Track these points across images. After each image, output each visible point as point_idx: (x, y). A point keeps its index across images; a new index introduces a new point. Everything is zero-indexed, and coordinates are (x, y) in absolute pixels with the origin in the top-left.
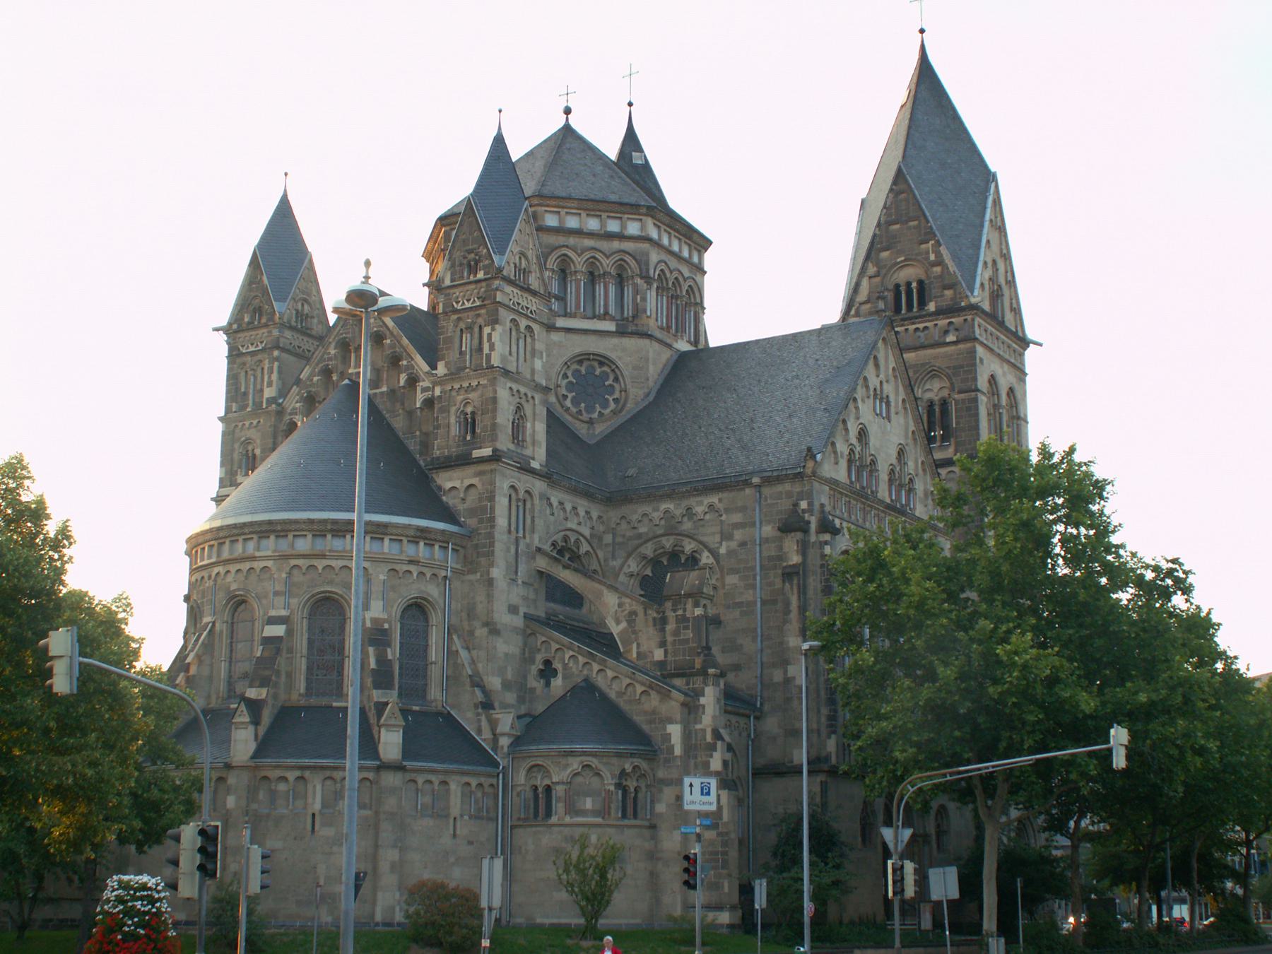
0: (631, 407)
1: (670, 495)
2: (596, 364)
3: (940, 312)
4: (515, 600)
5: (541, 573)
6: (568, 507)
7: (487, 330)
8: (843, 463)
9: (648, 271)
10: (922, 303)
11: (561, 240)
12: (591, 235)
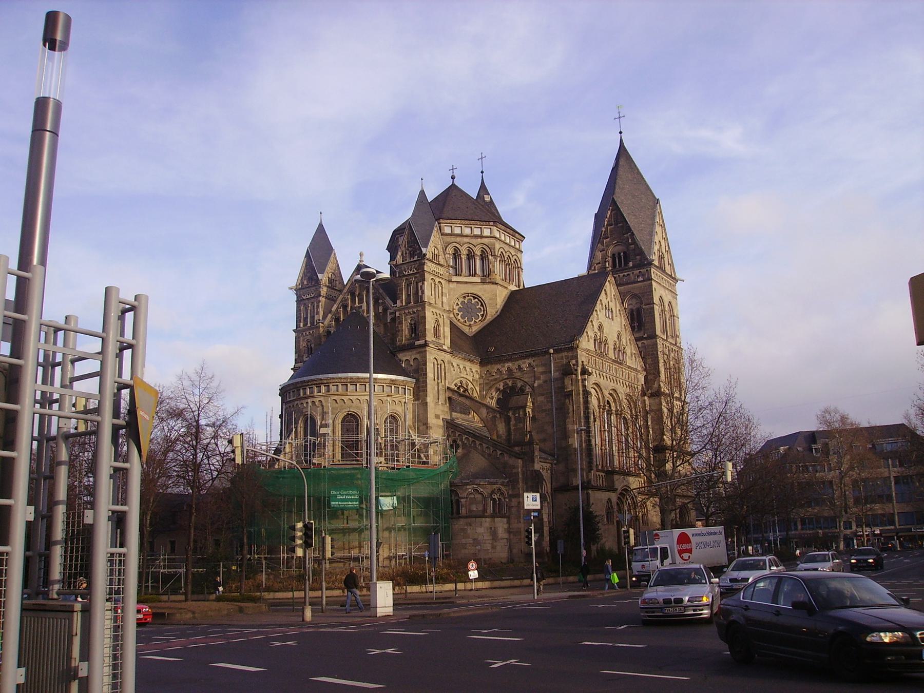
0: (489, 318)
1: (510, 360)
3: (634, 267)
4: (439, 413)
5: (609, 499)
6: (461, 367)
7: (420, 284)
8: (592, 341)
10: (626, 263)
11: (453, 239)
12: (467, 236)
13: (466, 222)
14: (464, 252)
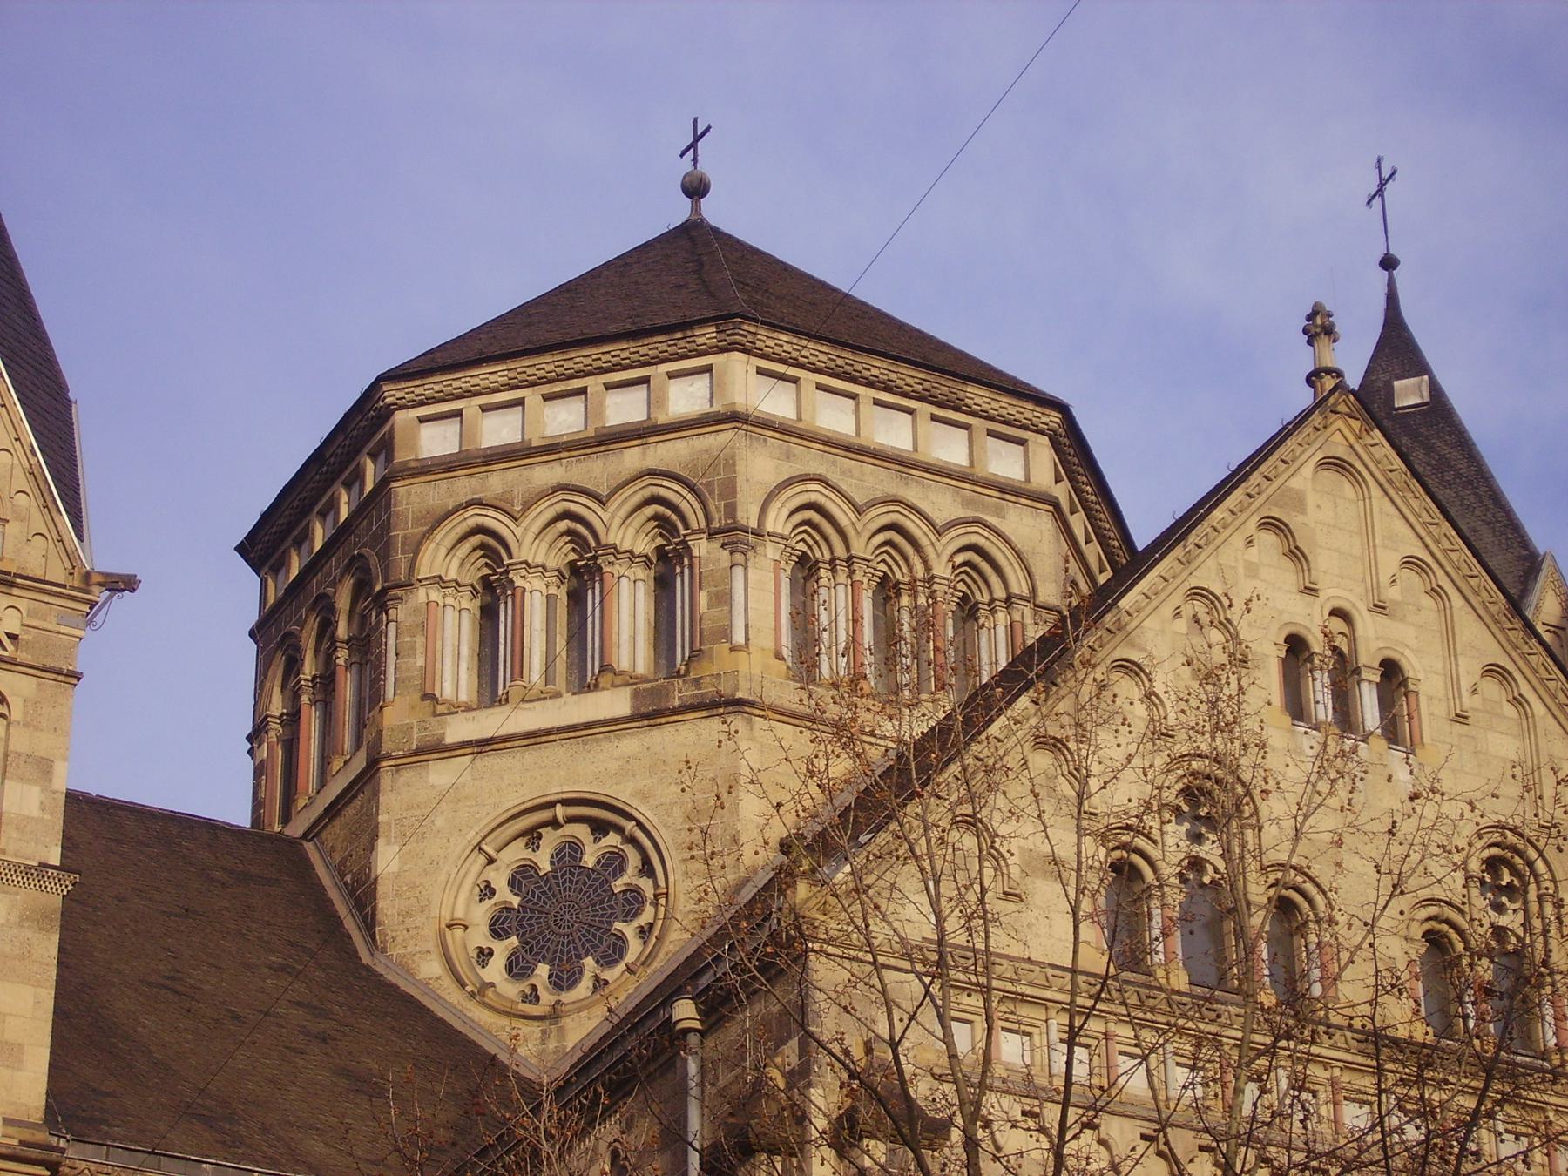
2: (582, 832)
9: (731, 510)
12: (553, 449)
13: (544, 364)
14: (537, 549)
